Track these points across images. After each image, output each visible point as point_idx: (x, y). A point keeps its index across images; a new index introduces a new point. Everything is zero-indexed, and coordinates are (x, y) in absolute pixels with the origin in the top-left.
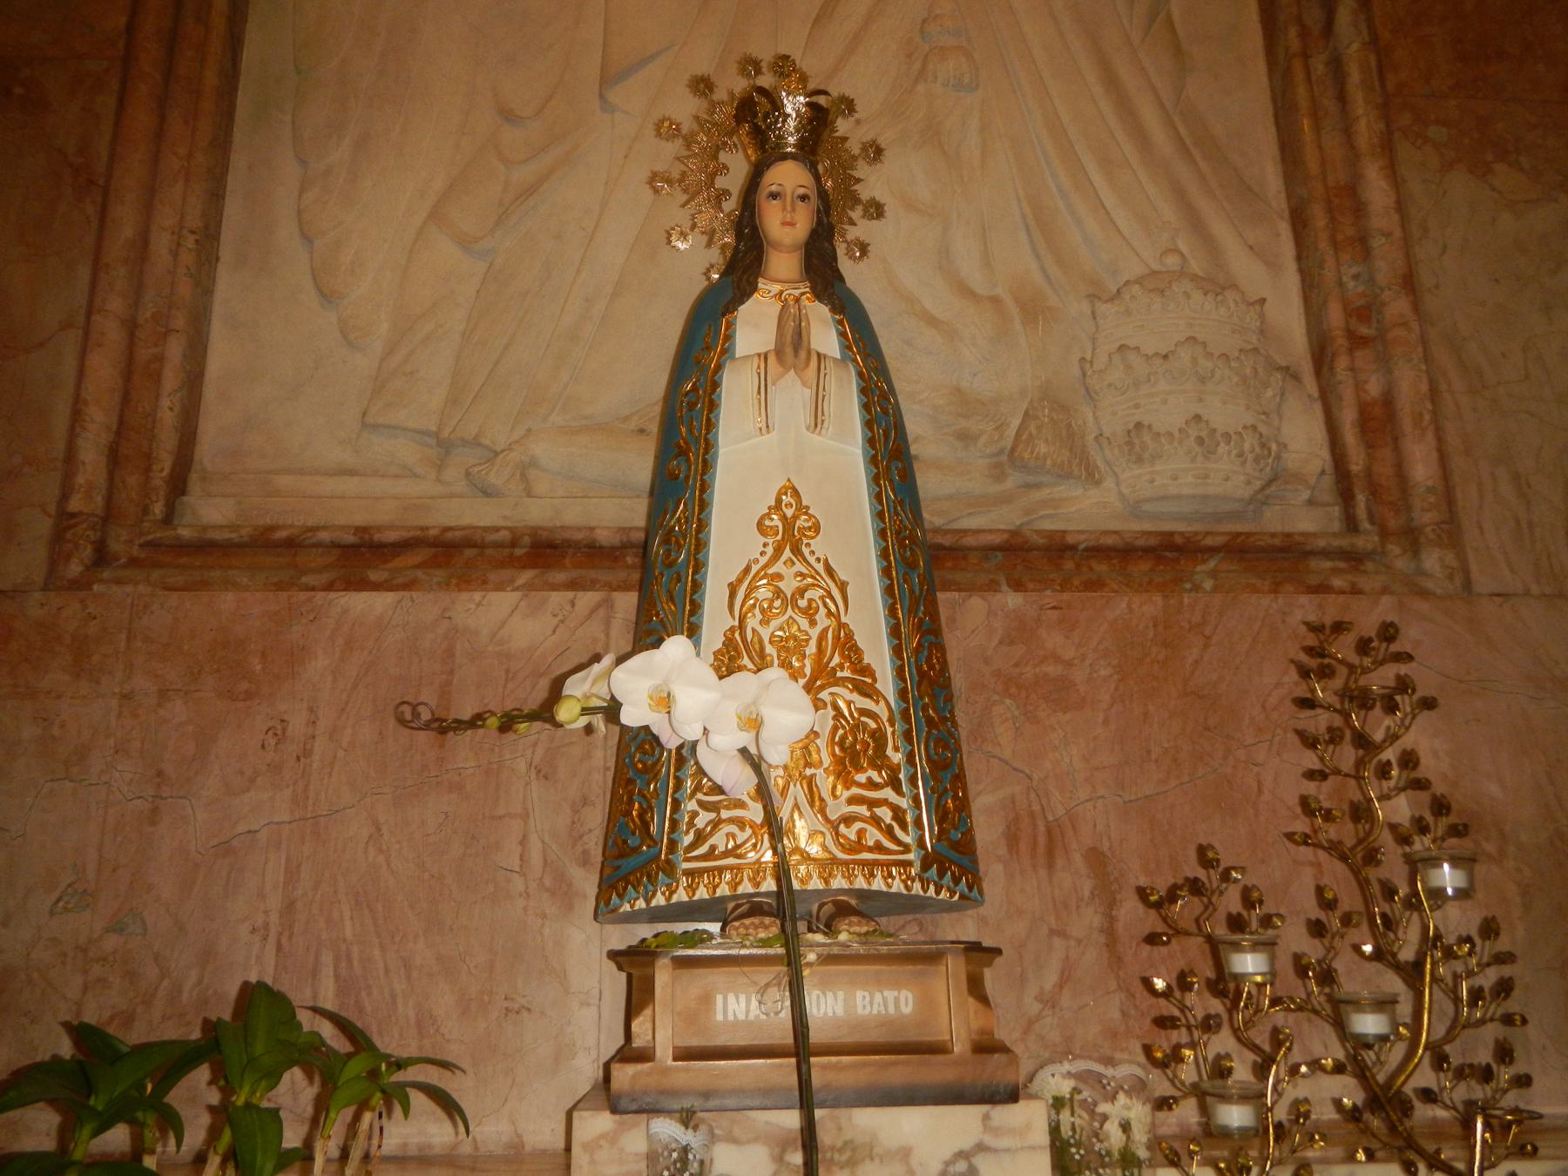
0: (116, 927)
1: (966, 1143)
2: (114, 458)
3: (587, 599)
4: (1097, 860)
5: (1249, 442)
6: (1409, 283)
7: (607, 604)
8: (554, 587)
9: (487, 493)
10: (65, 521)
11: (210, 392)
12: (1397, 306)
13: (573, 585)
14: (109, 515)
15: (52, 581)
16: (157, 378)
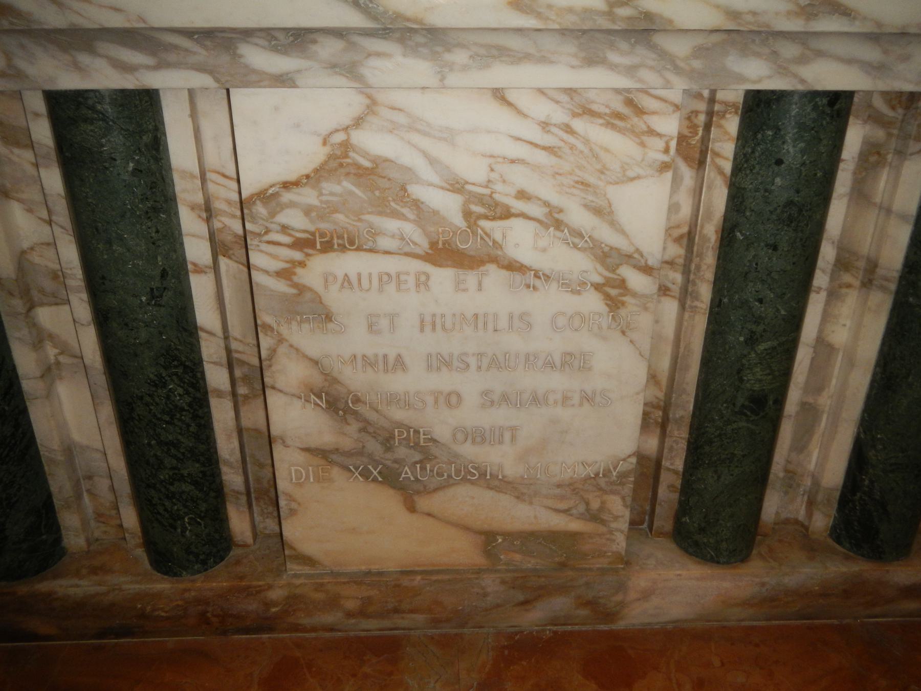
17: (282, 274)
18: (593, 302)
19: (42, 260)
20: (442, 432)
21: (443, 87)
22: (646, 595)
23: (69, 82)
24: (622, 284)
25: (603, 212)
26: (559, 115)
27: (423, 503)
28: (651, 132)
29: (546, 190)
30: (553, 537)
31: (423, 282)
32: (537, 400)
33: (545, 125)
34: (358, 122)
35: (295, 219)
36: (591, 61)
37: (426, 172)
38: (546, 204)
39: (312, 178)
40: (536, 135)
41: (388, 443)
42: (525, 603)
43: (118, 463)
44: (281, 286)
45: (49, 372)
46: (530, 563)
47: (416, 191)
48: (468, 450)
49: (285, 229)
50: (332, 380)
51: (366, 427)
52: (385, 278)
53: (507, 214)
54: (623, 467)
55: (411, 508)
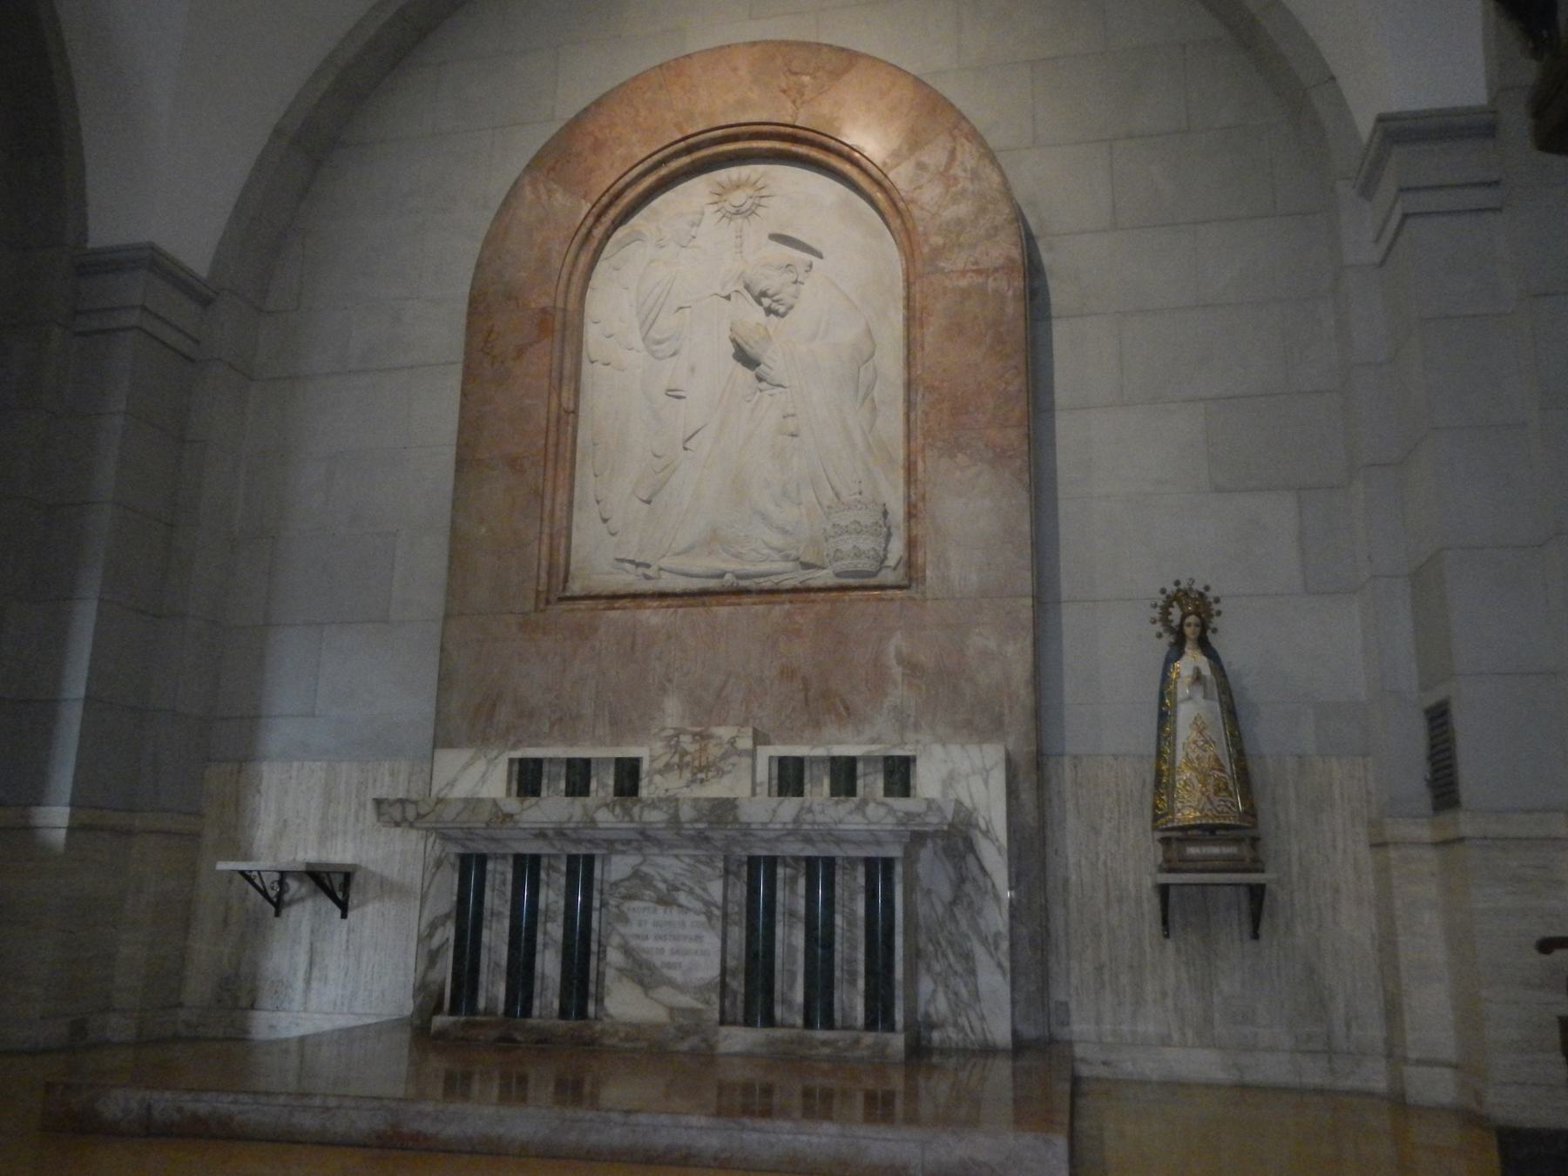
0: (557, 697)
1: (734, 735)
2: (549, 574)
3: (672, 610)
4: (804, 679)
5: (872, 553)
6: (923, 497)
7: (676, 612)
8: (663, 607)
9: (647, 577)
10: (538, 593)
11: (573, 552)
12: (920, 505)
13: (668, 607)
14: (549, 590)
15: (536, 609)
16: (559, 550)
17: (618, 907)
18: (703, 918)
19: (553, 907)
20: (658, 964)
21: (662, 855)
22: (726, 1037)
23: (574, 852)
24: (711, 912)
25: (705, 890)
26: (692, 862)
27: (651, 993)
28: (716, 867)
29: (687, 882)
30: (693, 1011)
31: (655, 911)
32: (686, 953)
33: (689, 865)
34: (641, 864)
35: (623, 890)
36: (697, 848)
37: (658, 877)
38: (689, 887)
39: (628, 879)
40: (686, 867)
41: (640, 966)
42: (682, 1038)
43: (558, 979)
44: (614, 910)
45: (545, 945)
46: (685, 1023)
47: (655, 882)
48: (665, 971)
49: (619, 893)
50: (627, 943)
51: (635, 960)
52: (645, 909)
53: (677, 889)
54: (716, 981)
55: (646, 995)
